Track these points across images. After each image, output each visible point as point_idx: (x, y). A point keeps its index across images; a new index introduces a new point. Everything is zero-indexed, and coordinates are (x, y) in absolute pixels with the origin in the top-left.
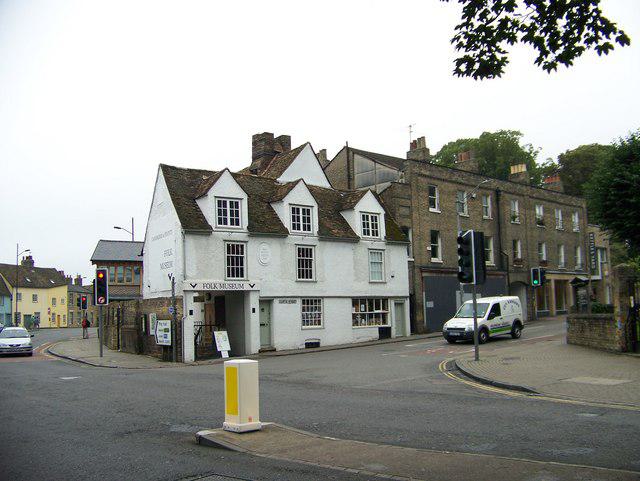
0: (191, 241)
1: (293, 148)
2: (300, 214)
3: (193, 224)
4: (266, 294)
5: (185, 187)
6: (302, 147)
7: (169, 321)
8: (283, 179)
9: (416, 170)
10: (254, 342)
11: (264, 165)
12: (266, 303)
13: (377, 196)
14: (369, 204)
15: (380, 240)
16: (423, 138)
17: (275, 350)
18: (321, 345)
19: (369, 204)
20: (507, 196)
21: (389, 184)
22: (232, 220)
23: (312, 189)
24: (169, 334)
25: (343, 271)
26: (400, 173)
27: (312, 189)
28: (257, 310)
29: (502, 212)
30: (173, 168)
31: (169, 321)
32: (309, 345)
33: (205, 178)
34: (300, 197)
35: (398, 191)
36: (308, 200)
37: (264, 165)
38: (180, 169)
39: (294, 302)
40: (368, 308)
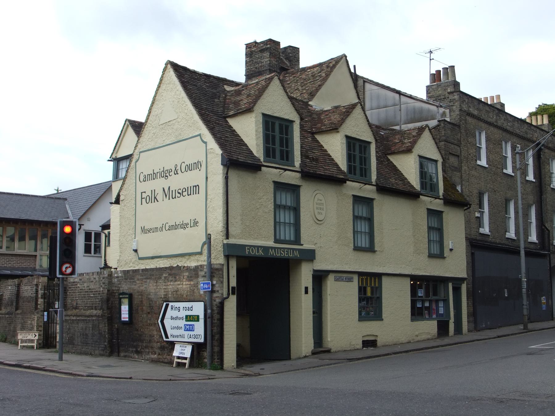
0: (234, 175)
4: (320, 265)
7: (202, 304)
9: (465, 107)
10: (302, 340)
15: (437, 198)
16: (453, 67)
18: (379, 344)
19: (427, 147)
20: (546, 151)
29: (543, 171)
31: (202, 304)
36: (367, 135)
38: (194, 72)
39: (350, 280)
40: (426, 292)
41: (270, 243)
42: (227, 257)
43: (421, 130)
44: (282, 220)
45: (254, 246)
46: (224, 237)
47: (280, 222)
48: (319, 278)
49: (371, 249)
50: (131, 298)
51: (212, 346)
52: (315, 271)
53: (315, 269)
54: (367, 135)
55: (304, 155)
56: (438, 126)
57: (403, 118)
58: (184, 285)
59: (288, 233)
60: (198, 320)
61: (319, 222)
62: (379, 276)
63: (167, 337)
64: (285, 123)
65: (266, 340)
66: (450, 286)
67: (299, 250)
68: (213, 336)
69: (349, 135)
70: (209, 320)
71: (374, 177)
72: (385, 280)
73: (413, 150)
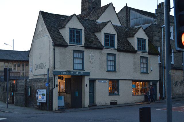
0: (57, 49)
1: (102, 6)
2: (109, 37)
3: (58, 43)
4: (92, 77)
5: (51, 22)
6: (108, 5)
7: (46, 90)
8: (100, 21)
10: (86, 102)
11: (88, 14)
12: (92, 82)
13: (145, 31)
14: (141, 34)
17: (96, 106)
18: (118, 103)
19: (141, 34)
21: (149, 25)
23: (115, 27)
24: (45, 97)
25: (128, 66)
26: (154, 19)
27: (115, 27)
28: (88, 85)
30: (47, 13)
31: (46, 90)
32: (112, 103)
33: (62, 19)
34: (109, 29)
35: (154, 28)
36: (113, 32)
37: (88, 14)
41: (72, 70)
42: (54, 75)
43: (139, 28)
44: (77, 62)
45: (65, 71)
46: (53, 69)
47: (76, 63)
48: (92, 82)
49: (115, 71)
50: (31, 88)
51: (49, 104)
52: (90, 79)
53: (90, 78)
54: (113, 32)
55: (86, 40)
56: (150, 26)
57: (142, 23)
58: (43, 84)
59: (80, 67)
60: (45, 95)
61: (92, 63)
62: (118, 80)
63: (38, 101)
64: (78, 30)
65: (74, 102)
67: (83, 72)
68: (49, 100)
69: (105, 32)
70: (48, 95)
71: (116, 46)
72: (120, 81)
73: (134, 36)
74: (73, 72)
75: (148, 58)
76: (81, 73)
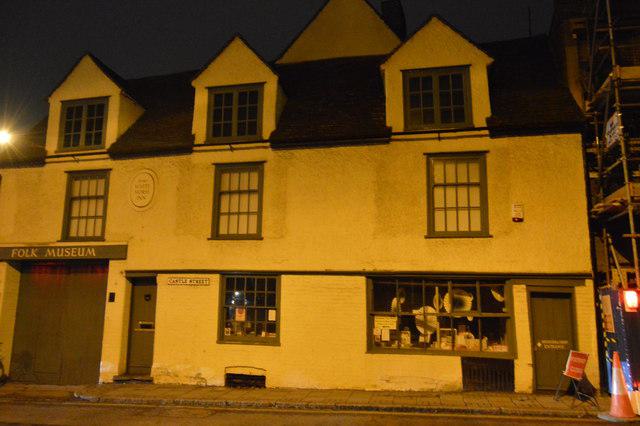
4: (137, 262)
17: (150, 381)
18: (269, 383)
22: (88, 137)
32: (233, 380)
45: (24, 248)
48: (143, 283)
66: (520, 295)
74: (55, 248)
75: (489, 158)
76: (89, 250)
